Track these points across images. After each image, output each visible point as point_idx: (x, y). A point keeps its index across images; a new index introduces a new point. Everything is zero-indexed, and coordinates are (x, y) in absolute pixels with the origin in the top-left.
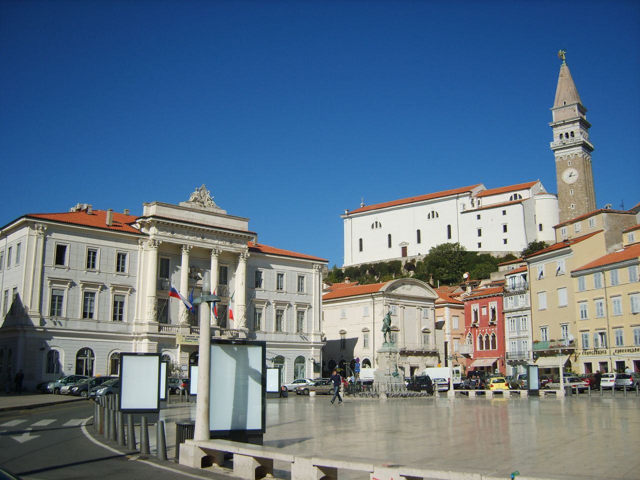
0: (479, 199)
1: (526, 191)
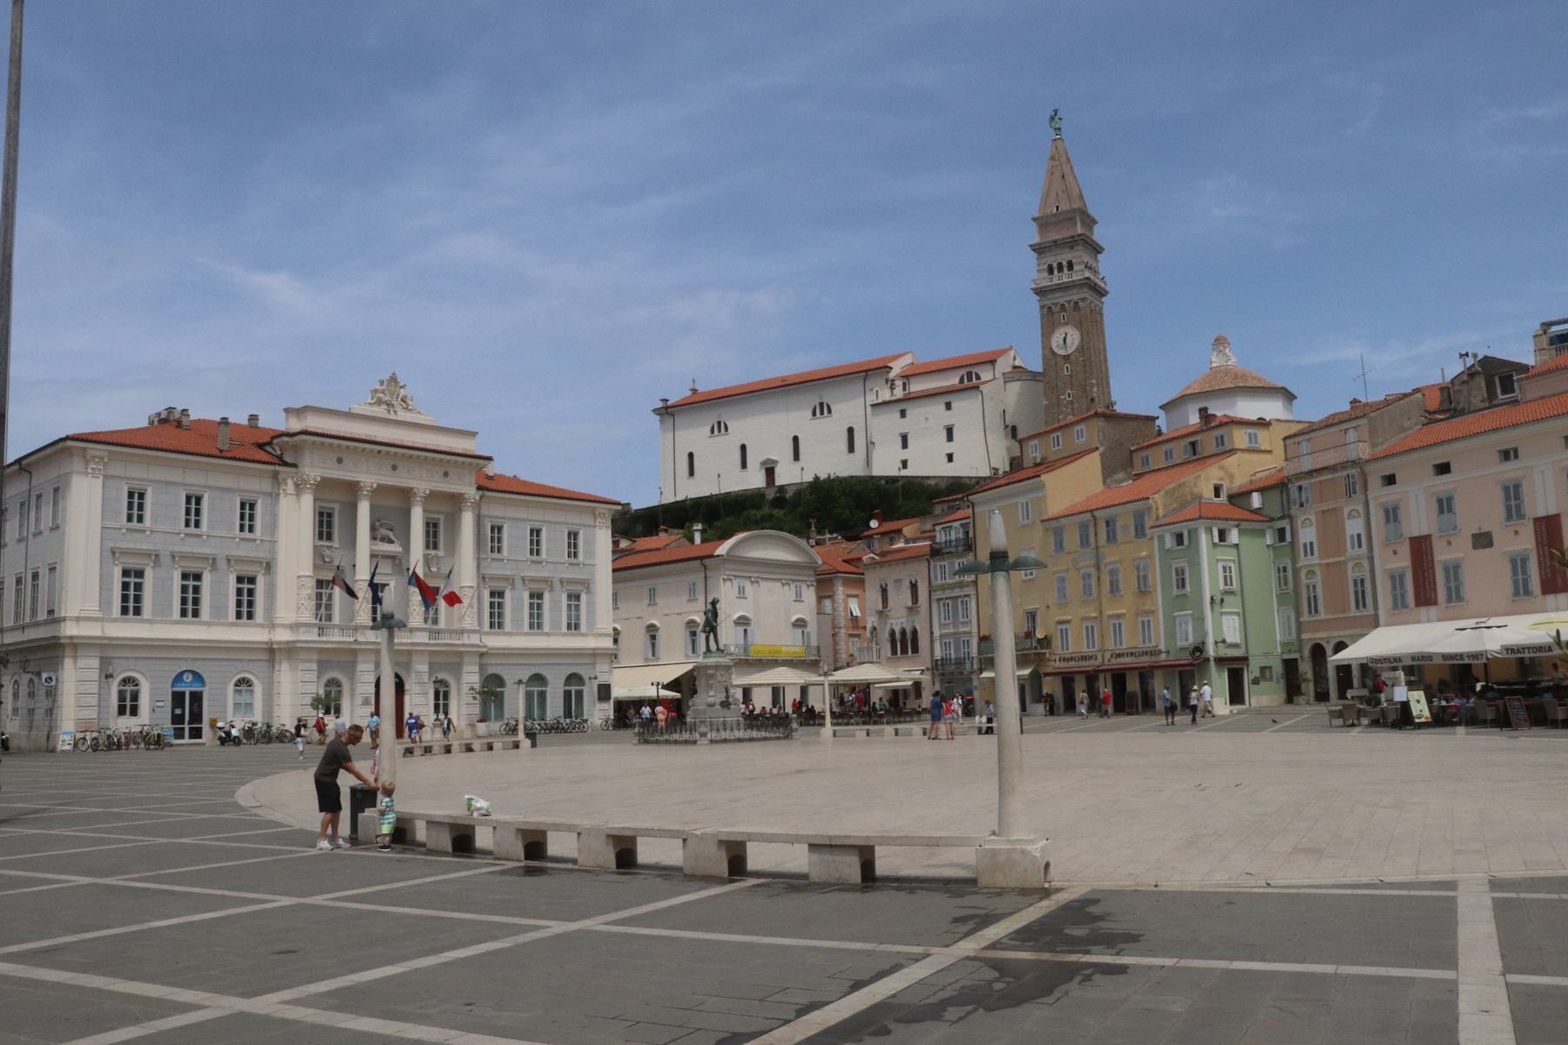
1: (989, 367)
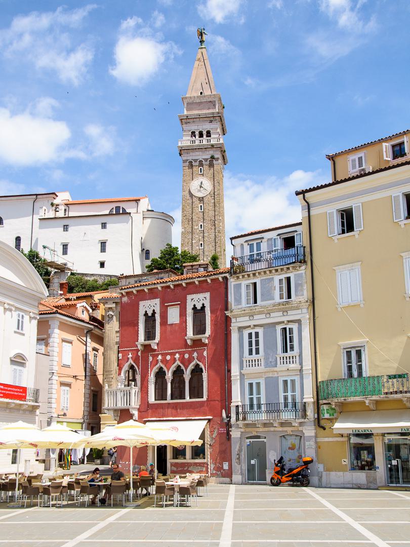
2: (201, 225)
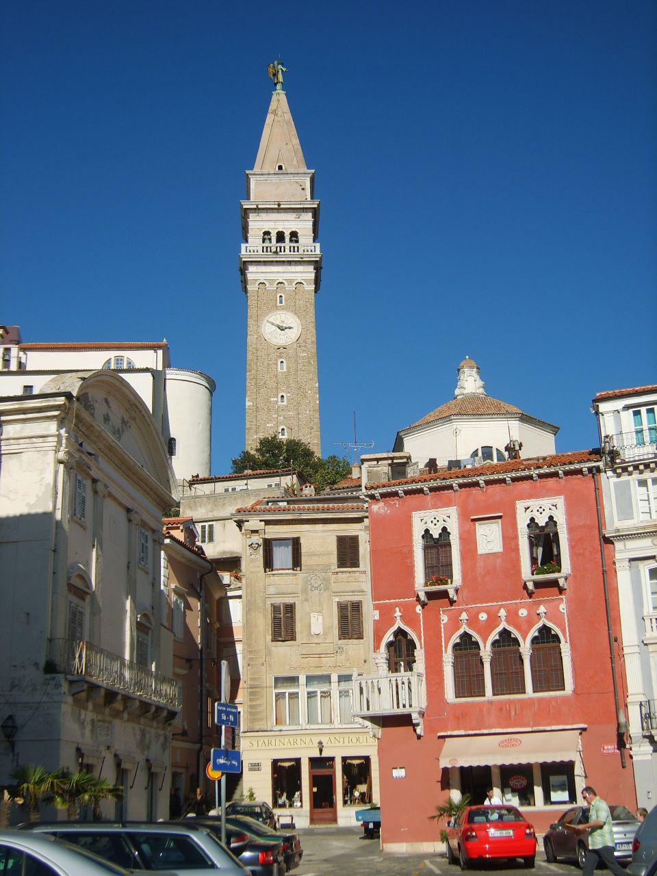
0: (21, 354)
1: (150, 354)
2: (282, 396)
